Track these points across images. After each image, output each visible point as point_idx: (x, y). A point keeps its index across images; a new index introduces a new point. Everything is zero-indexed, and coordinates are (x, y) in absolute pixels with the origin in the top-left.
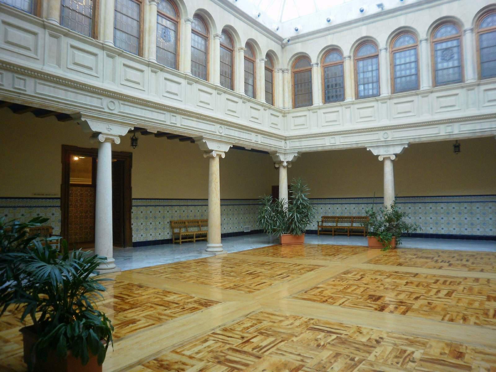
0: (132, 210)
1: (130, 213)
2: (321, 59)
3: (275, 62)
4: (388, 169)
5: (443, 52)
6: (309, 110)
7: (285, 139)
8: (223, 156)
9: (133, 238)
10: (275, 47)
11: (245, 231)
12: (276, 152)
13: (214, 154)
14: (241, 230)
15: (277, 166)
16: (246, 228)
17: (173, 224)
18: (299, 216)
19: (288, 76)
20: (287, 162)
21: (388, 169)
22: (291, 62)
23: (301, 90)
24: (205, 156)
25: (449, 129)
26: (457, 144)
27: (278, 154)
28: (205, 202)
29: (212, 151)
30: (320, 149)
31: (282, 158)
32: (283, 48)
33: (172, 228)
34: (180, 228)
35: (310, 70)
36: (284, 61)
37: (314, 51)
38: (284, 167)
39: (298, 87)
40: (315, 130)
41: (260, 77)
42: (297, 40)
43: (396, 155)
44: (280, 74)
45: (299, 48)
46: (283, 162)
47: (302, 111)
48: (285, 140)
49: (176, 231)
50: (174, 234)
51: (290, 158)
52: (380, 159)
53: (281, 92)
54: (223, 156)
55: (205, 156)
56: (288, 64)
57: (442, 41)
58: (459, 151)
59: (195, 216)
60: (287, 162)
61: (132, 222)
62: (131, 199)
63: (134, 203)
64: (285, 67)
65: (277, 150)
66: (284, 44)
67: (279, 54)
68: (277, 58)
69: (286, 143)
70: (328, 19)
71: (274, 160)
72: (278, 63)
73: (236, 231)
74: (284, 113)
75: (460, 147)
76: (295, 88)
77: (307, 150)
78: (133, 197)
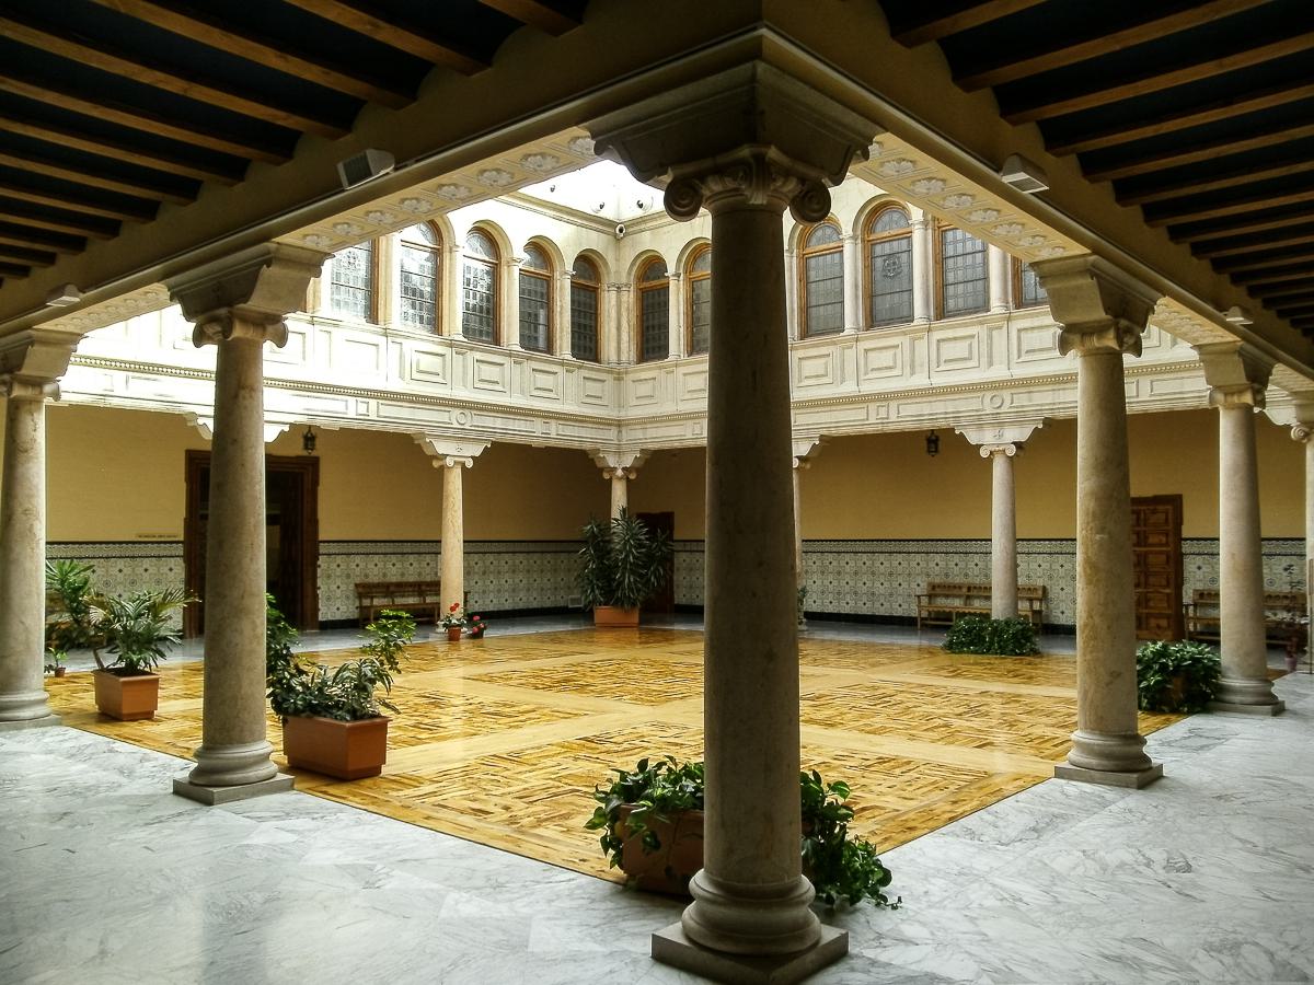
0: (319, 563)
1: (315, 566)
2: (686, 264)
3: (602, 270)
5: (885, 261)
6: (660, 368)
7: (619, 424)
9: (320, 613)
10: (595, 241)
11: (570, 606)
14: (561, 603)
15: (606, 476)
16: (572, 600)
17: (365, 590)
18: (632, 580)
19: (630, 298)
20: (624, 469)
22: (635, 268)
23: (653, 327)
25: (861, 414)
26: (934, 438)
28: (434, 546)
30: (677, 445)
31: (611, 461)
32: (618, 240)
33: (360, 596)
34: (372, 598)
35: (666, 288)
36: (620, 268)
38: (620, 479)
39: (648, 319)
40: (669, 408)
41: (561, 307)
42: (643, 226)
44: (613, 294)
46: (615, 468)
47: (650, 370)
48: (619, 426)
49: (366, 602)
50: (361, 608)
51: (628, 461)
53: (614, 331)
56: (629, 274)
57: (883, 241)
58: (936, 451)
59: (420, 574)
60: (624, 469)
61: (319, 583)
62: (316, 542)
63: (323, 548)
64: (624, 281)
65: (599, 446)
67: (610, 257)
68: (606, 264)
69: (620, 432)
71: (599, 465)
72: (608, 273)
73: (548, 604)
74: (619, 373)
75: (940, 443)
76: (642, 321)
77: (656, 446)
78: (322, 537)
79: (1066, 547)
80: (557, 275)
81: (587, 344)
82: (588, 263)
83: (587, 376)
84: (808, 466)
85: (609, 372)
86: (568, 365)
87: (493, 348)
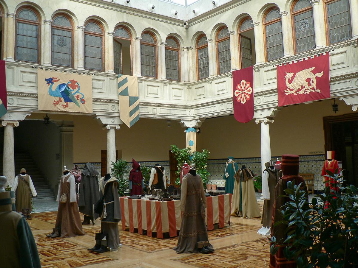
4: (265, 130)
8: (118, 128)
12: (180, 120)
13: (108, 127)
21: (265, 130)
24: (103, 129)
27: (182, 122)
29: (106, 125)
37: (208, 28)
43: (270, 118)
45: (195, 28)
52: (257, 122)
54: (118, 128)
55: (104, 129)
66: (187, 25)
70: (214, 2)
79: (257, 160)
80: (159, 45)
81: (174, 74)
82: (173, 38)
83: (149, 84)
84: (273, 121)
85: (185, 85)
86: (164, 83)
87: (155, 79)
